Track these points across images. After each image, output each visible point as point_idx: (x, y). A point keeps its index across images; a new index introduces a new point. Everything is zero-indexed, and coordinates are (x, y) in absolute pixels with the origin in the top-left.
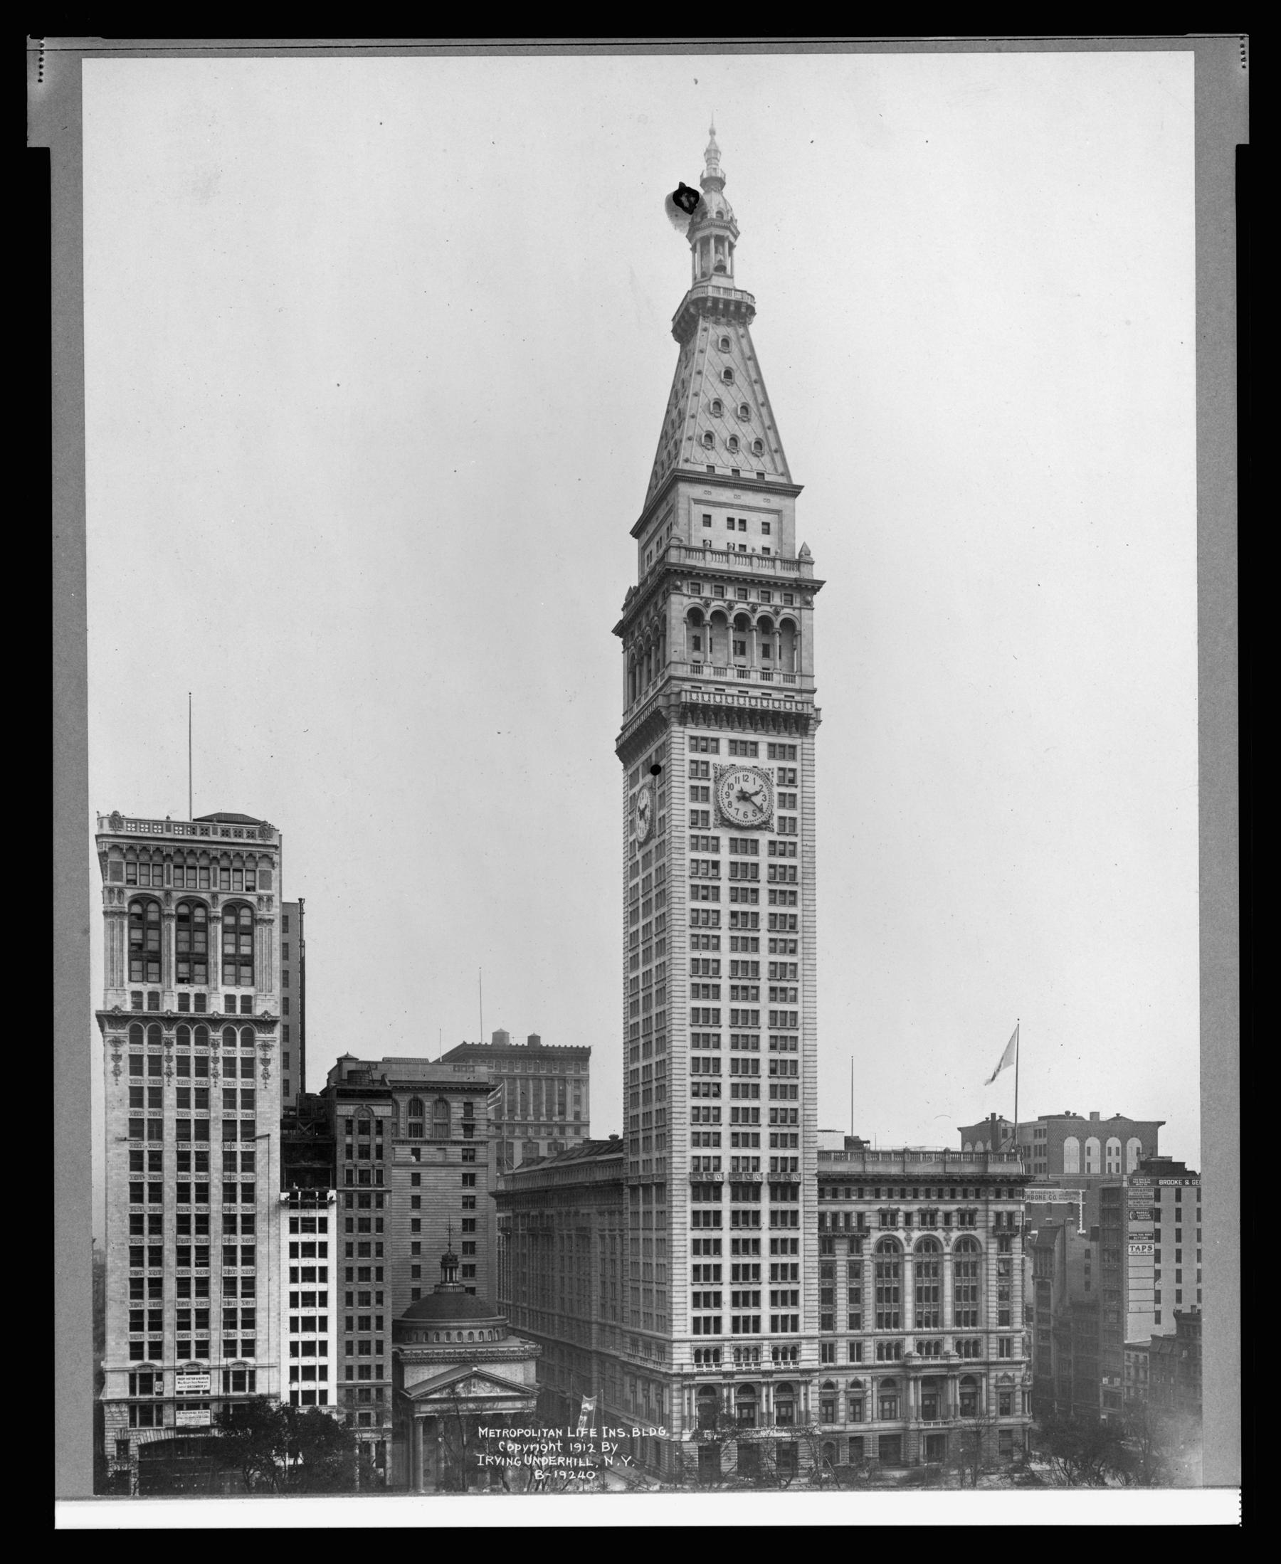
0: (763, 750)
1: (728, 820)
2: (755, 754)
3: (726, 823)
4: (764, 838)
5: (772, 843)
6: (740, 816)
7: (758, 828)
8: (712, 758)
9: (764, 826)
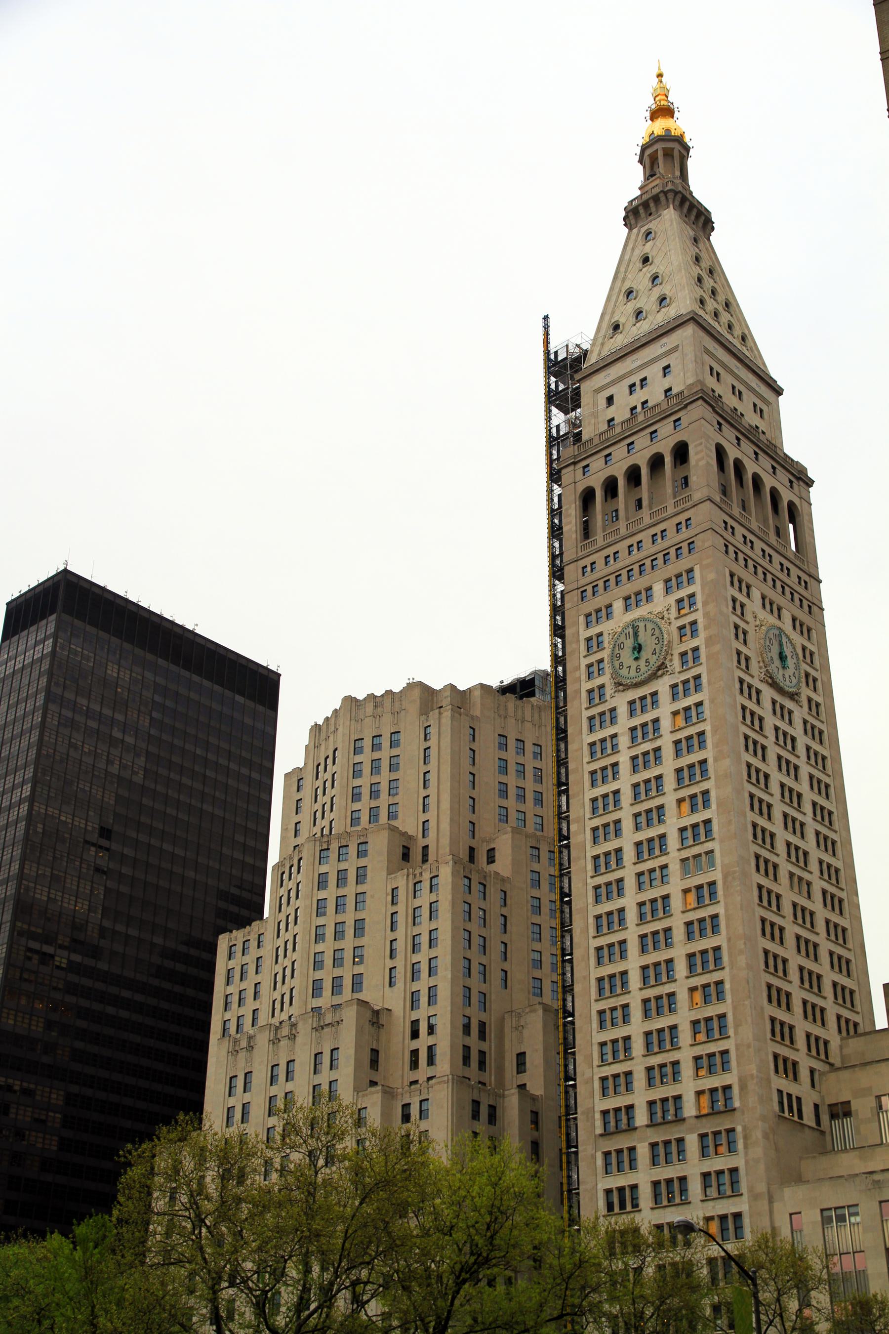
0: (658, 588)
1: (620, 684)
2: (649, 598)
3: (621, 686)
4: (662, 686)
5: (674, 686)
6: (633, 673)
7: (654, 676)
8: (607, 627)
9: (660, 670)
